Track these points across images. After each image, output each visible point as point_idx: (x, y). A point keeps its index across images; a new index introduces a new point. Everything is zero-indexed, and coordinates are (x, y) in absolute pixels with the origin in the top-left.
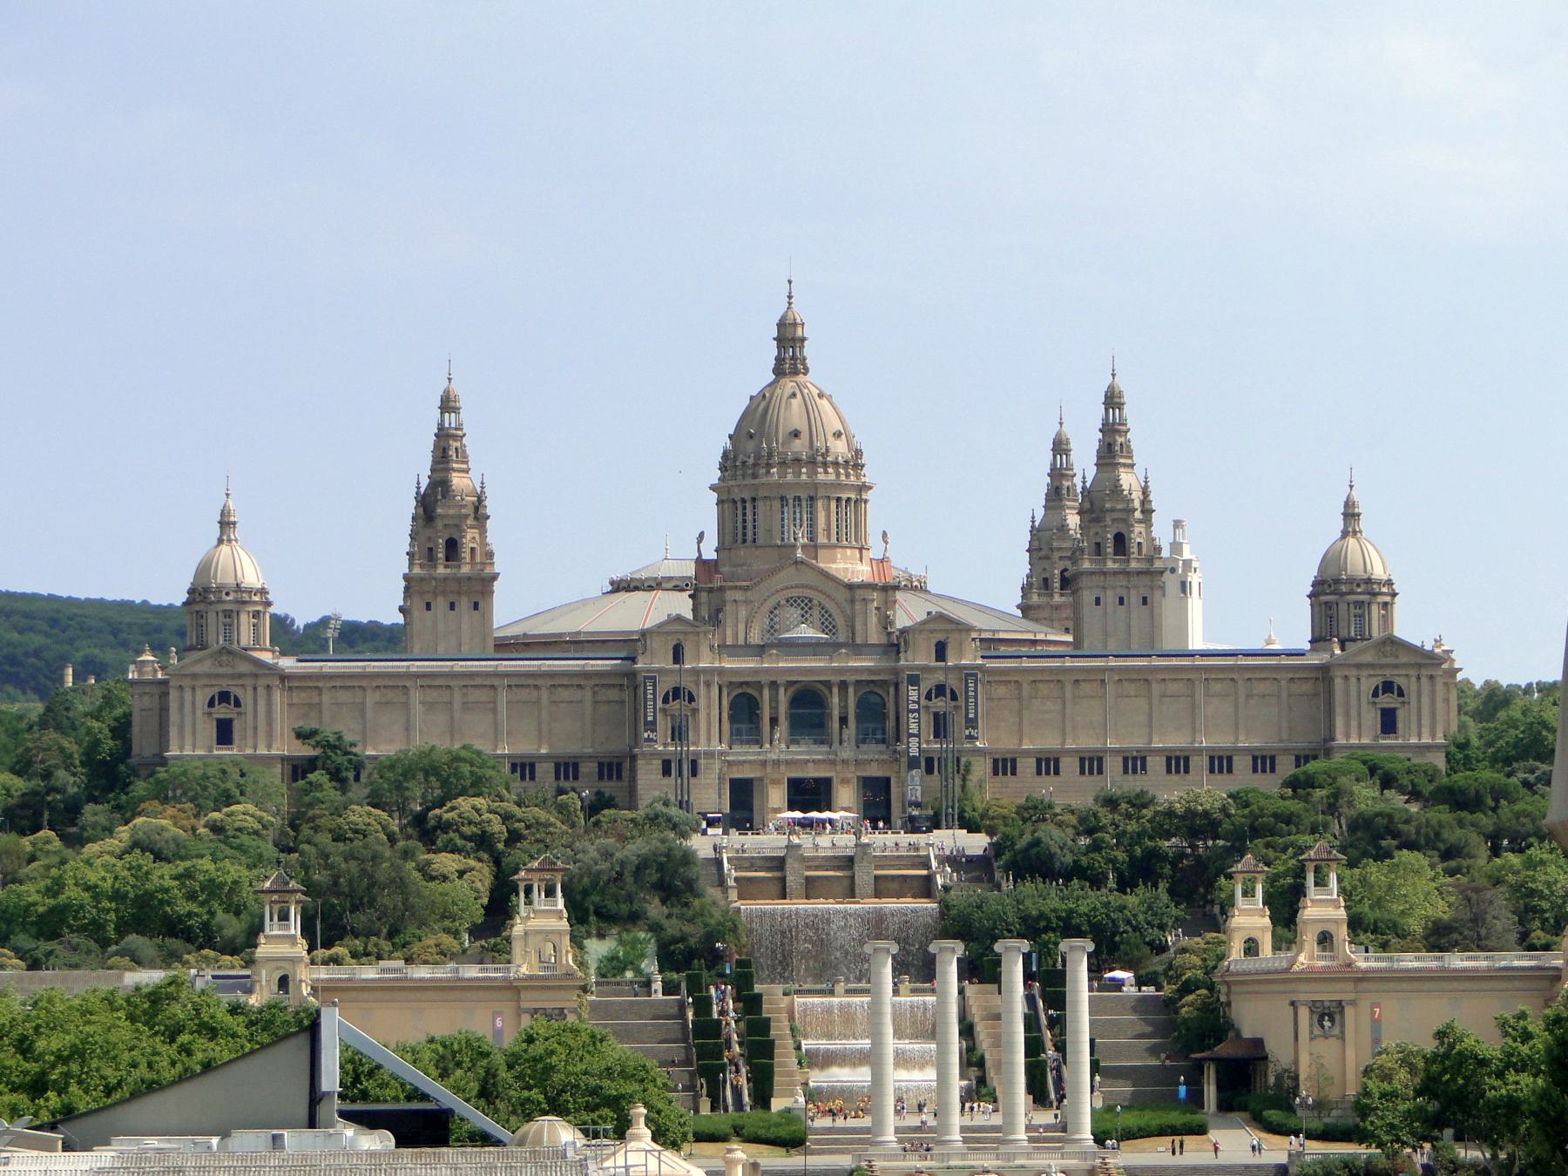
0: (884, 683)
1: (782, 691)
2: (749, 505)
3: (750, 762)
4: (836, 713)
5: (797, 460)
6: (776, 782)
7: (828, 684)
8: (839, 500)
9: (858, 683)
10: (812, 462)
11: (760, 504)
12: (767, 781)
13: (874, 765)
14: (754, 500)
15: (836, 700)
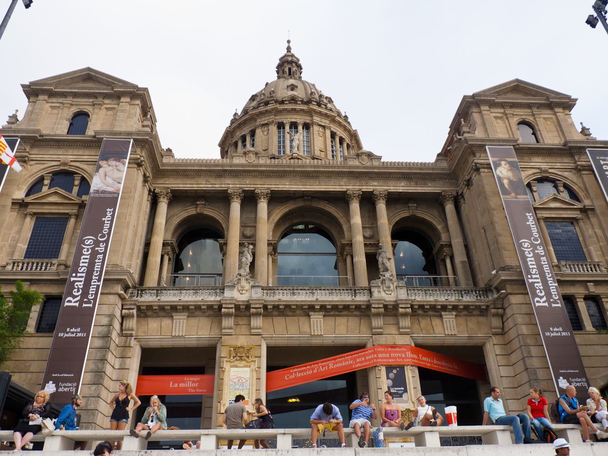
0: (436, 201)
1: (263, 206)
2: (248, 138)
3: (186, 308)
4: (359, 239)
5: (293, 100)
6: (241, 355)
7: (342, 199)
8: (333, 135)
9: (393, 200)
10: (308, 102)
11: (259, 132)
12: (222, 352)
13: (449, 318)
14: (253, 133)
15: (357, 219)
